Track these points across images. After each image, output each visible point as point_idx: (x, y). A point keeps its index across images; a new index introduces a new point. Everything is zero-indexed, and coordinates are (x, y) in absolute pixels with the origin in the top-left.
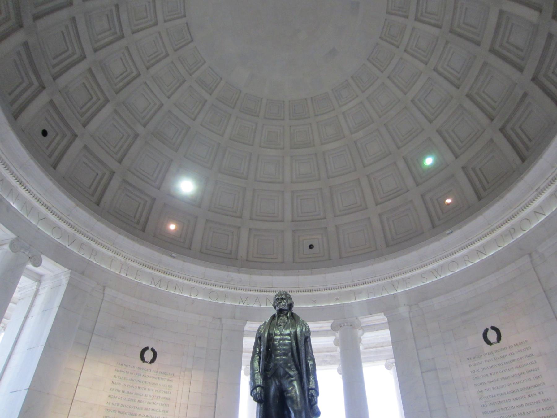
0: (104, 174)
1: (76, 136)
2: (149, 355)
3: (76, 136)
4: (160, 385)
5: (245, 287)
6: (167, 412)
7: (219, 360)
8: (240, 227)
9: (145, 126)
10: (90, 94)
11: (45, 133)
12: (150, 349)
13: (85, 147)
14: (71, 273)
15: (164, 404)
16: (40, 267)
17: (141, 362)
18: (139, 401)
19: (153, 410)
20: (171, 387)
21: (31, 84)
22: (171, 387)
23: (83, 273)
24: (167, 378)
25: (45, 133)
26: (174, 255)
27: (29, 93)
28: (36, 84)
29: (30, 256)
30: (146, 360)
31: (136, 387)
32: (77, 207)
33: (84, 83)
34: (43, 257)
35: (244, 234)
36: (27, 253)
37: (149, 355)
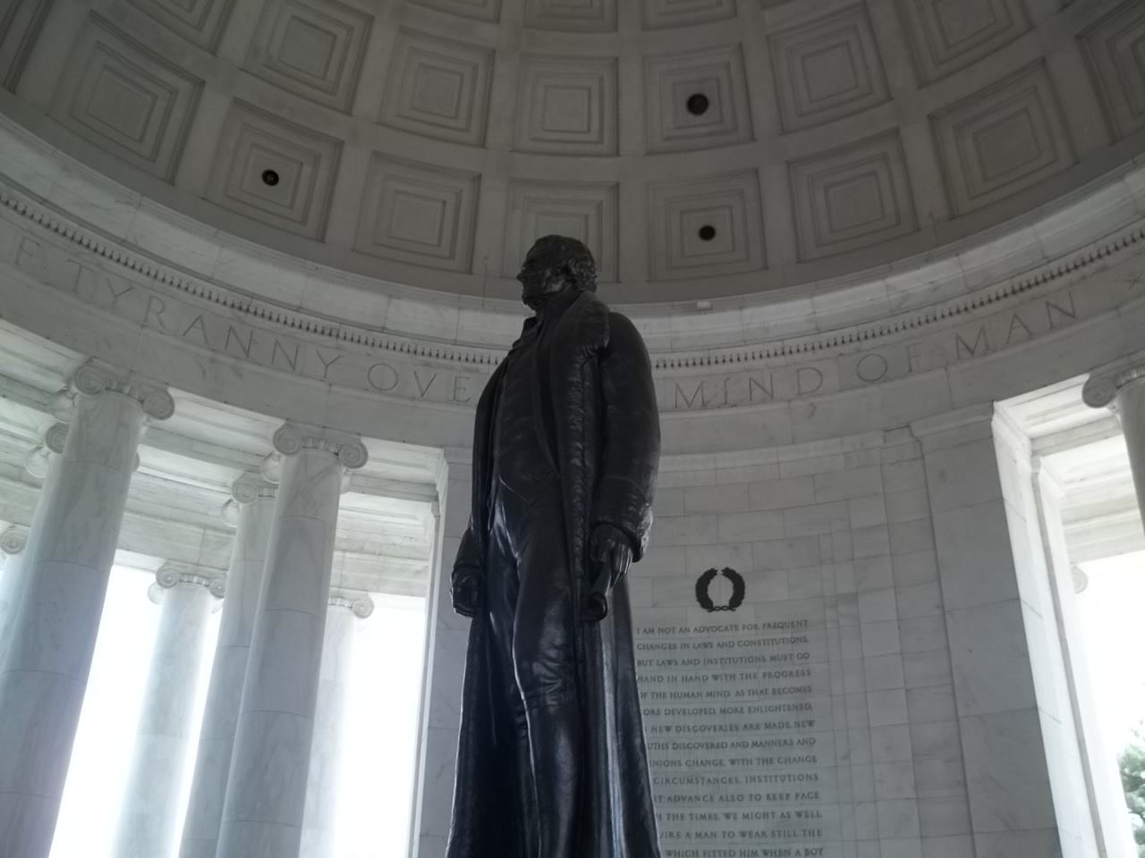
1: (341, 144)
2: (721, 591)
3: (341, 144)
4: (773, 658)
5: (961, 302)
6: (811, 723)
7: (935, 548)
8: (897, 131)
9: (497, 20)
10: (328, 33)
11: (271, 178)
12: (720, 572)
13: (378, 156)
14: (445, 455)
15: (796, 707)
16: (369, 462)
17: (705, 611)
18: (724, 711)
19: (768, 726)
20: (805, 656)
21: (174, 92)
22: (805, 656)
24: (789, 636)
25: (271, 178)
26: (704, 304)
27: (178, 113)
28: (183, 86)
29: (333, 449)
30: (715, 604)
31: (705, 679)
33: (294, 17)
34: (366, 441)
35: (918, 142)
36: (322, 444)
37: (721, 591)
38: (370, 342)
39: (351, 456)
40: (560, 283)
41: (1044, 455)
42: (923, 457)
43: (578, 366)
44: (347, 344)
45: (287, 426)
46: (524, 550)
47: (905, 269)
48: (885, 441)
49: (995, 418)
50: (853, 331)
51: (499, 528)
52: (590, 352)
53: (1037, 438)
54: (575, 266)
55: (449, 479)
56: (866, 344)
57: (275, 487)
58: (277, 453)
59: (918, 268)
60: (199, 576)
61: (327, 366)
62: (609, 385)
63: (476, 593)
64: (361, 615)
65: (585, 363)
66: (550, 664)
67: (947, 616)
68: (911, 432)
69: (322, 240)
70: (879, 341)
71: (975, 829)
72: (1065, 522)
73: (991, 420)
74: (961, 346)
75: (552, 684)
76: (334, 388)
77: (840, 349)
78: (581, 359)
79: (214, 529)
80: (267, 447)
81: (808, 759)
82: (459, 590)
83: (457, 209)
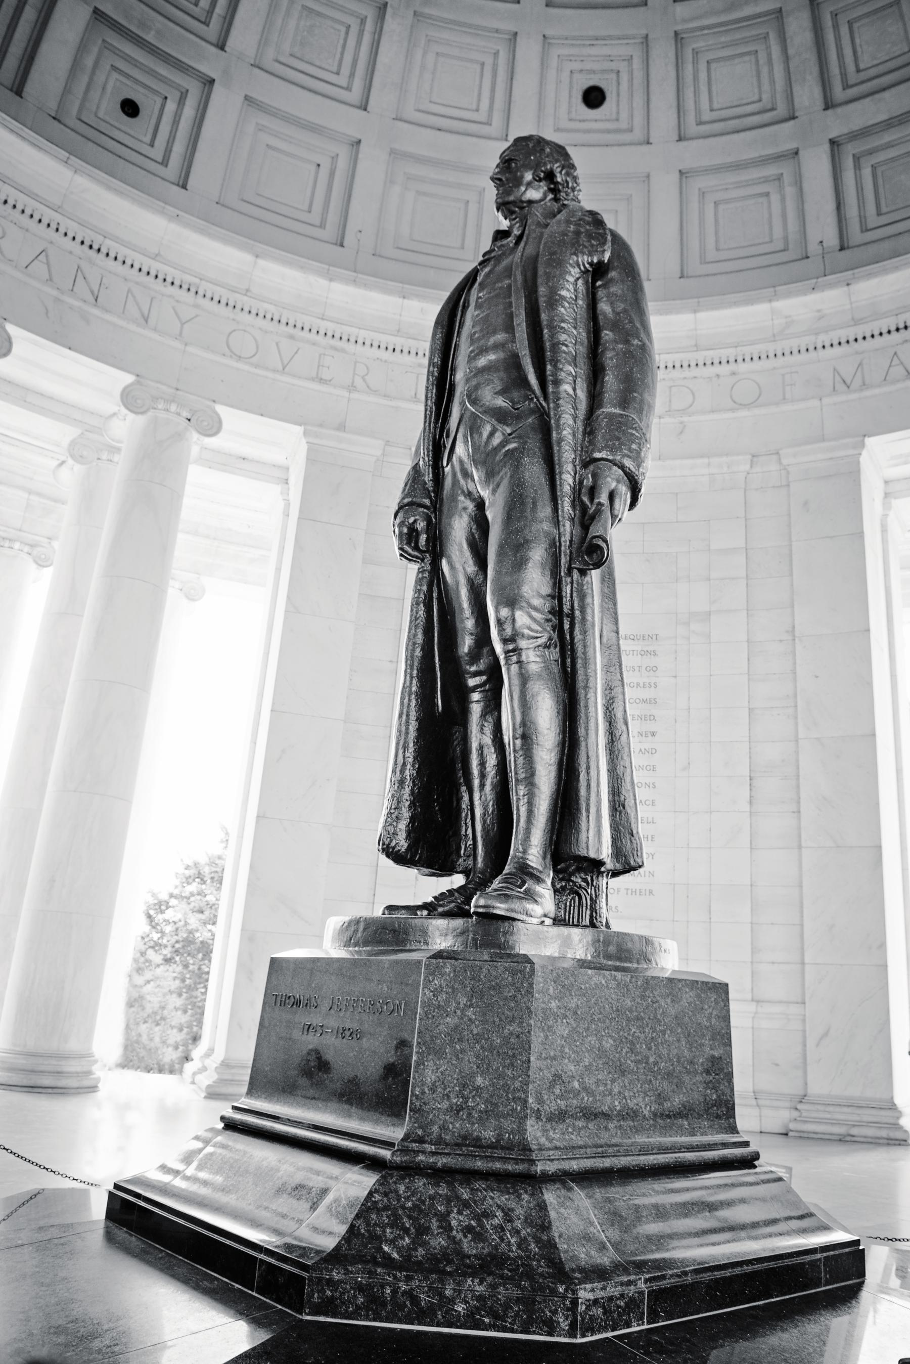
0: (334, 159)
7: (791, 575)
14: (306, 434)
16: (221, 434)
23: (342, 427)
29: (186, 414)
32: (261, 262)
34: (221, 409)
35: (817, 166)
36: (173, 408)
38: (231, 304)
39: (205, 423)
40: (542, 191)
41: (895, 498)
42: (788, 485)
43: (572, 279)
44: (206, 303)
45: (138, 383)
46: (498, 486)
47: (788, 295)
48: (751, 467)
49: (864, 453)
50: (731, 353)
51: (461, 462)
52: (587, 266)
53: (891, 481)
54: (561, 172)
55: (307, 459)
56: (742, 367)
57: (119, 450)
58: (124, 411)
59: (805, 295)
60: (21, 542)
61: (183, 324)
62: (604, 307)
63: (425, 536)
64: (191, 598)
65: (578, 279)
66: (534, 614)
67: (797, 641)
68: (780, 459)
69: (184, 187)
70: (757, 365)
71: (803, 844)
72: (902, 568)
73: (860, 454)
74: (838, 379)
75: (537, 638)
76: (190, 349)
77: (717, 369)
78: (575, 272)
79: (39, 494)
80: (112, 405)
81: (648, 768)
82: (405, 530)
83: (332, 174)
